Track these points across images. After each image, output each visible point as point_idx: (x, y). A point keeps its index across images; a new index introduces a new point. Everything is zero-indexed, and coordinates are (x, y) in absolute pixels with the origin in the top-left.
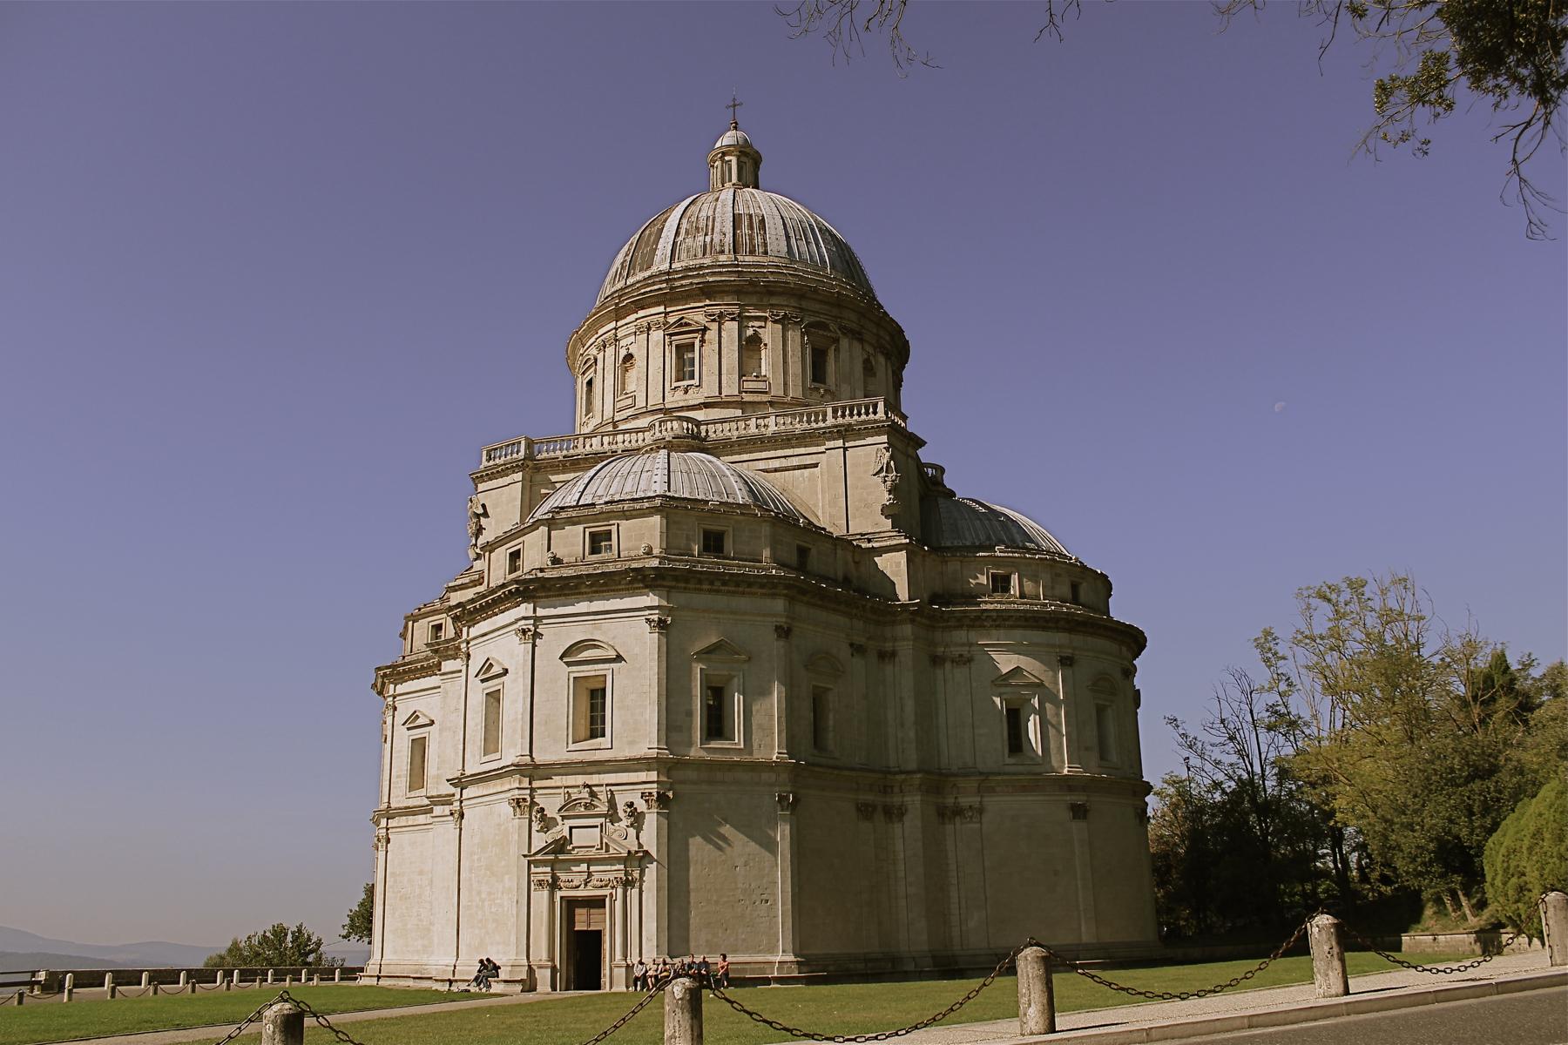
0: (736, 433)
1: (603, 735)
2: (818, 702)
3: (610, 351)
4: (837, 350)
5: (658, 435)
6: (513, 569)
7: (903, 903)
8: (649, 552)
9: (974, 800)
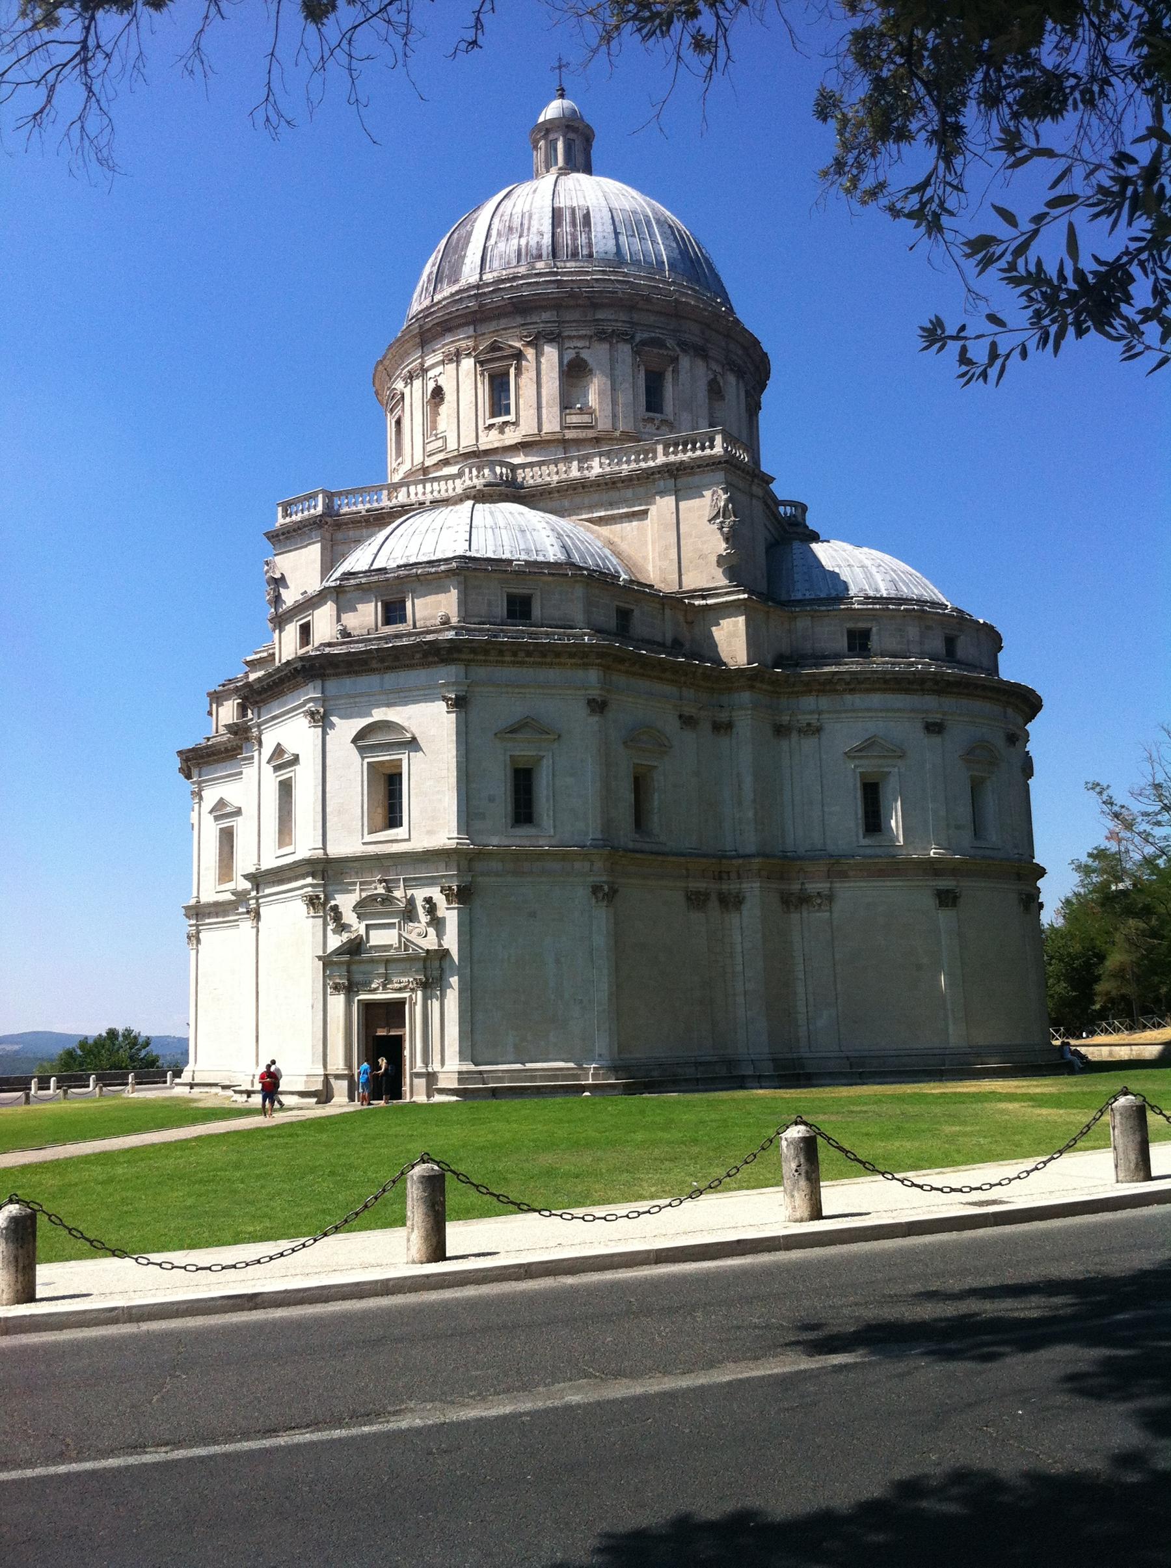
0: (556, 478)
1: (401, 825)
2: (640, 784)
3: (417, 383)
4: (676, 371)
5: (468, 483)
7: (740, 999)
8: (446, 621)
9: (823, 886)
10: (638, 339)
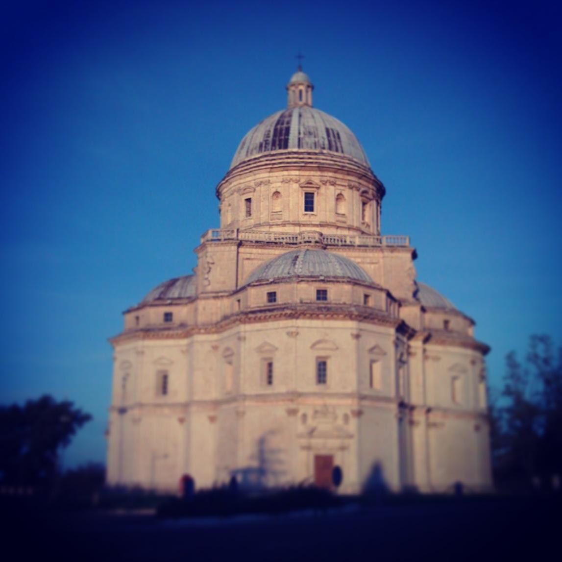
3: (263, 188)
5: (307, 239)
6: (270, 301)
10: (361, 191)
